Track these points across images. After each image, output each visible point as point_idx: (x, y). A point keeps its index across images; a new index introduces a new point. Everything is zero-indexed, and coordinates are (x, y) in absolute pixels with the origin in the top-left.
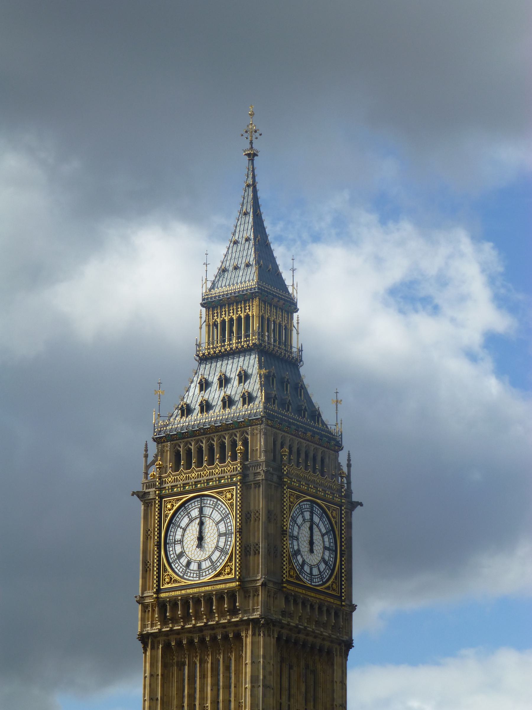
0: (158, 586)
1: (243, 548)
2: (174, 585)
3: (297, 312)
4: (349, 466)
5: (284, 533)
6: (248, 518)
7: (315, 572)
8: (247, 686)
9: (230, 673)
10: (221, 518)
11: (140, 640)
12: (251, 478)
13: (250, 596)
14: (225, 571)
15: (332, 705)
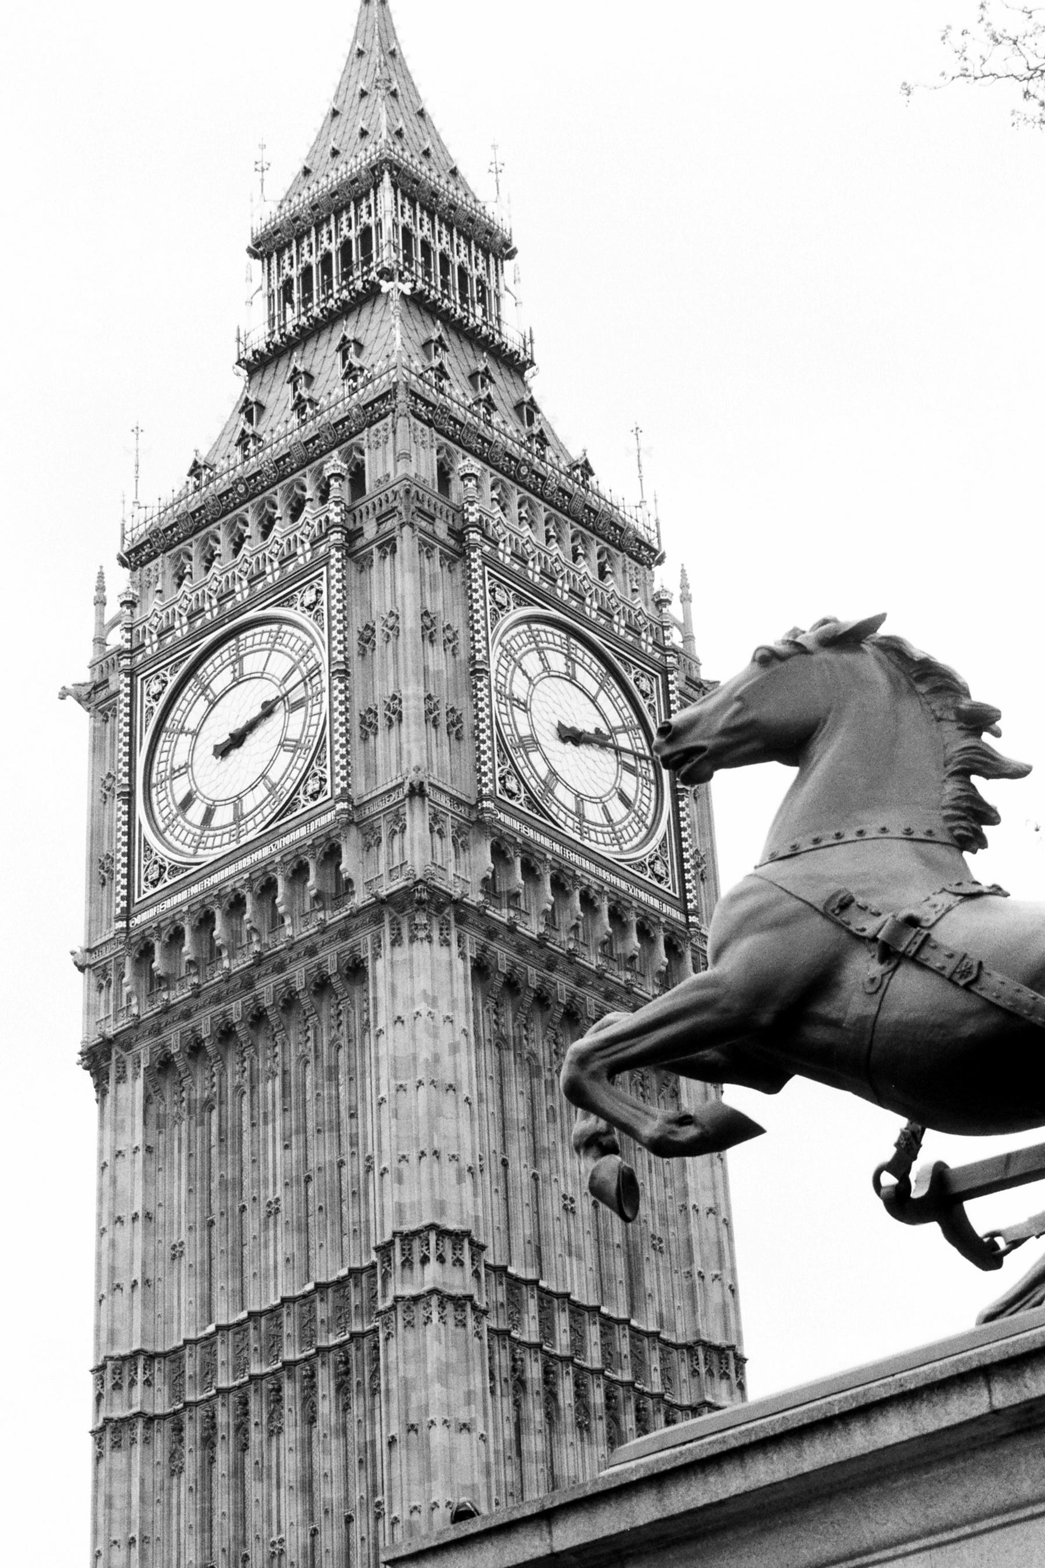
0: (128, 898)
1: (357, 721)
2: (170, 882)
3: (510, 256)
4: (685, 599)
5: (477, 671)
6: (367, 642)
7: (593, 812)
8: (384, 1093)
9: (338, 1085)
10: (292, 663)
11: (86, 1068)
12: (370, 530)
13: (379, 840)
14: (305, 793)
15: (684, 1207)
